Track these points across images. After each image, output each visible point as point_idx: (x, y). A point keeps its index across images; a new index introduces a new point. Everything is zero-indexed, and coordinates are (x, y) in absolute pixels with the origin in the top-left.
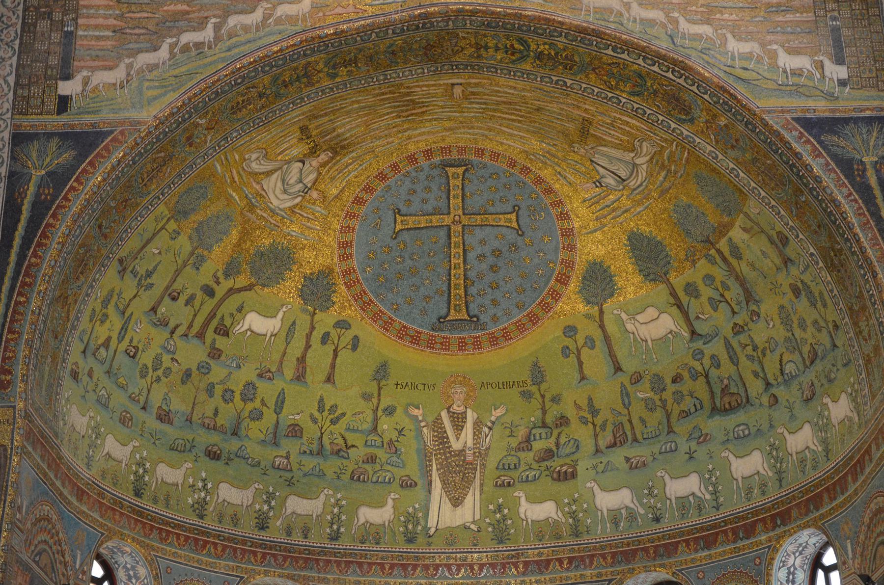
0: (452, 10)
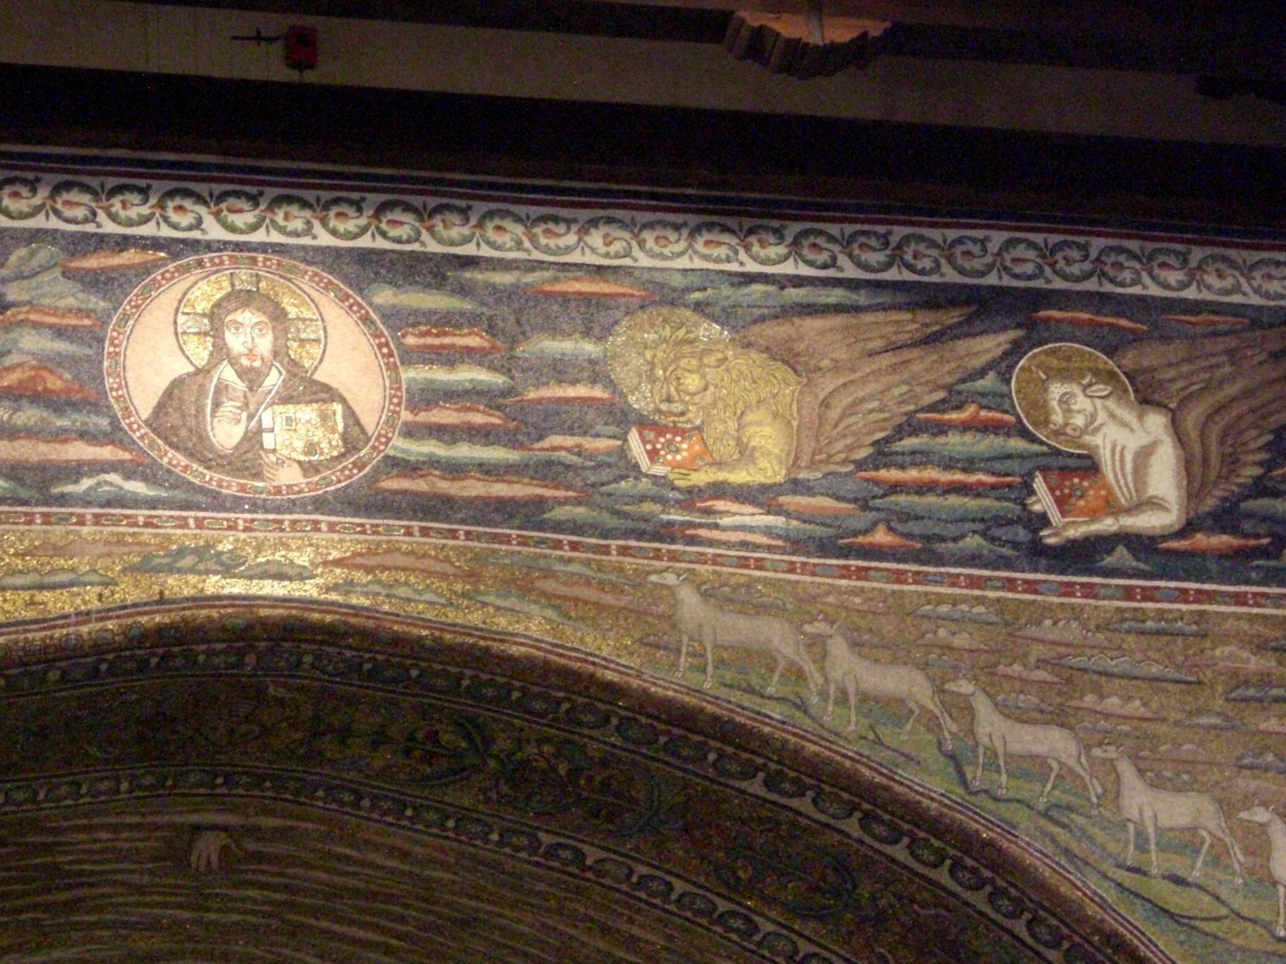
0: (264, 623)
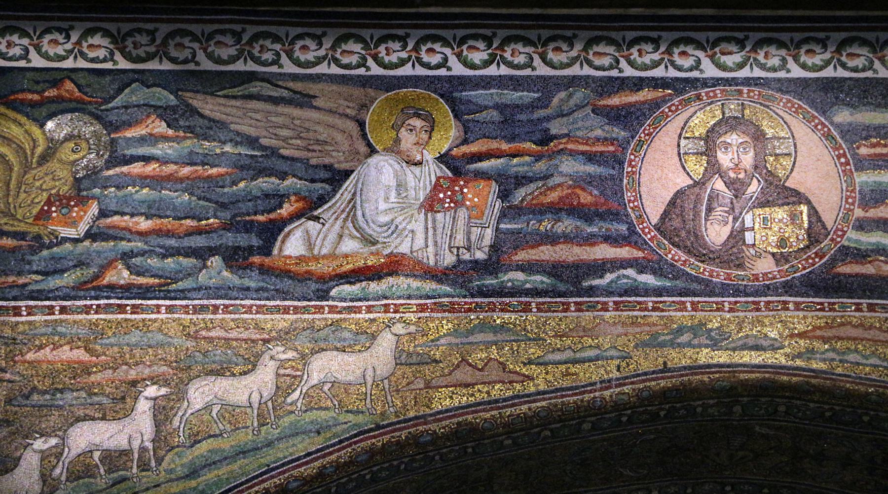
0: (744, 383)
